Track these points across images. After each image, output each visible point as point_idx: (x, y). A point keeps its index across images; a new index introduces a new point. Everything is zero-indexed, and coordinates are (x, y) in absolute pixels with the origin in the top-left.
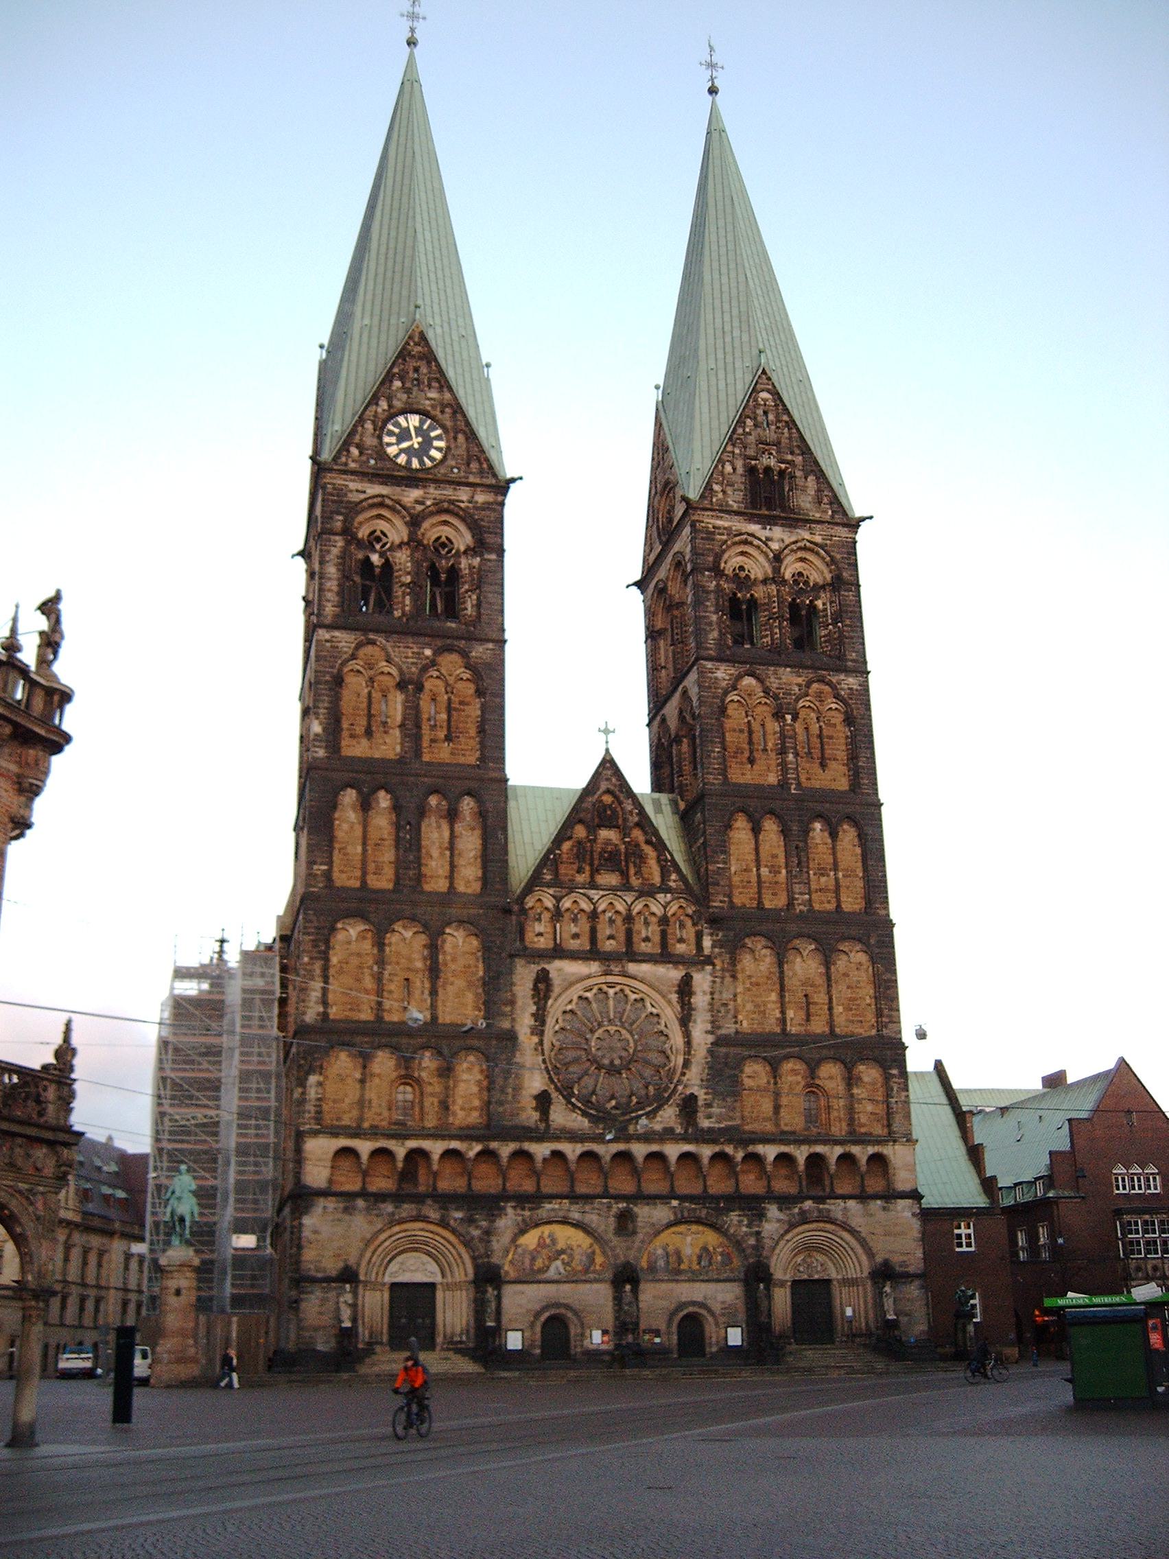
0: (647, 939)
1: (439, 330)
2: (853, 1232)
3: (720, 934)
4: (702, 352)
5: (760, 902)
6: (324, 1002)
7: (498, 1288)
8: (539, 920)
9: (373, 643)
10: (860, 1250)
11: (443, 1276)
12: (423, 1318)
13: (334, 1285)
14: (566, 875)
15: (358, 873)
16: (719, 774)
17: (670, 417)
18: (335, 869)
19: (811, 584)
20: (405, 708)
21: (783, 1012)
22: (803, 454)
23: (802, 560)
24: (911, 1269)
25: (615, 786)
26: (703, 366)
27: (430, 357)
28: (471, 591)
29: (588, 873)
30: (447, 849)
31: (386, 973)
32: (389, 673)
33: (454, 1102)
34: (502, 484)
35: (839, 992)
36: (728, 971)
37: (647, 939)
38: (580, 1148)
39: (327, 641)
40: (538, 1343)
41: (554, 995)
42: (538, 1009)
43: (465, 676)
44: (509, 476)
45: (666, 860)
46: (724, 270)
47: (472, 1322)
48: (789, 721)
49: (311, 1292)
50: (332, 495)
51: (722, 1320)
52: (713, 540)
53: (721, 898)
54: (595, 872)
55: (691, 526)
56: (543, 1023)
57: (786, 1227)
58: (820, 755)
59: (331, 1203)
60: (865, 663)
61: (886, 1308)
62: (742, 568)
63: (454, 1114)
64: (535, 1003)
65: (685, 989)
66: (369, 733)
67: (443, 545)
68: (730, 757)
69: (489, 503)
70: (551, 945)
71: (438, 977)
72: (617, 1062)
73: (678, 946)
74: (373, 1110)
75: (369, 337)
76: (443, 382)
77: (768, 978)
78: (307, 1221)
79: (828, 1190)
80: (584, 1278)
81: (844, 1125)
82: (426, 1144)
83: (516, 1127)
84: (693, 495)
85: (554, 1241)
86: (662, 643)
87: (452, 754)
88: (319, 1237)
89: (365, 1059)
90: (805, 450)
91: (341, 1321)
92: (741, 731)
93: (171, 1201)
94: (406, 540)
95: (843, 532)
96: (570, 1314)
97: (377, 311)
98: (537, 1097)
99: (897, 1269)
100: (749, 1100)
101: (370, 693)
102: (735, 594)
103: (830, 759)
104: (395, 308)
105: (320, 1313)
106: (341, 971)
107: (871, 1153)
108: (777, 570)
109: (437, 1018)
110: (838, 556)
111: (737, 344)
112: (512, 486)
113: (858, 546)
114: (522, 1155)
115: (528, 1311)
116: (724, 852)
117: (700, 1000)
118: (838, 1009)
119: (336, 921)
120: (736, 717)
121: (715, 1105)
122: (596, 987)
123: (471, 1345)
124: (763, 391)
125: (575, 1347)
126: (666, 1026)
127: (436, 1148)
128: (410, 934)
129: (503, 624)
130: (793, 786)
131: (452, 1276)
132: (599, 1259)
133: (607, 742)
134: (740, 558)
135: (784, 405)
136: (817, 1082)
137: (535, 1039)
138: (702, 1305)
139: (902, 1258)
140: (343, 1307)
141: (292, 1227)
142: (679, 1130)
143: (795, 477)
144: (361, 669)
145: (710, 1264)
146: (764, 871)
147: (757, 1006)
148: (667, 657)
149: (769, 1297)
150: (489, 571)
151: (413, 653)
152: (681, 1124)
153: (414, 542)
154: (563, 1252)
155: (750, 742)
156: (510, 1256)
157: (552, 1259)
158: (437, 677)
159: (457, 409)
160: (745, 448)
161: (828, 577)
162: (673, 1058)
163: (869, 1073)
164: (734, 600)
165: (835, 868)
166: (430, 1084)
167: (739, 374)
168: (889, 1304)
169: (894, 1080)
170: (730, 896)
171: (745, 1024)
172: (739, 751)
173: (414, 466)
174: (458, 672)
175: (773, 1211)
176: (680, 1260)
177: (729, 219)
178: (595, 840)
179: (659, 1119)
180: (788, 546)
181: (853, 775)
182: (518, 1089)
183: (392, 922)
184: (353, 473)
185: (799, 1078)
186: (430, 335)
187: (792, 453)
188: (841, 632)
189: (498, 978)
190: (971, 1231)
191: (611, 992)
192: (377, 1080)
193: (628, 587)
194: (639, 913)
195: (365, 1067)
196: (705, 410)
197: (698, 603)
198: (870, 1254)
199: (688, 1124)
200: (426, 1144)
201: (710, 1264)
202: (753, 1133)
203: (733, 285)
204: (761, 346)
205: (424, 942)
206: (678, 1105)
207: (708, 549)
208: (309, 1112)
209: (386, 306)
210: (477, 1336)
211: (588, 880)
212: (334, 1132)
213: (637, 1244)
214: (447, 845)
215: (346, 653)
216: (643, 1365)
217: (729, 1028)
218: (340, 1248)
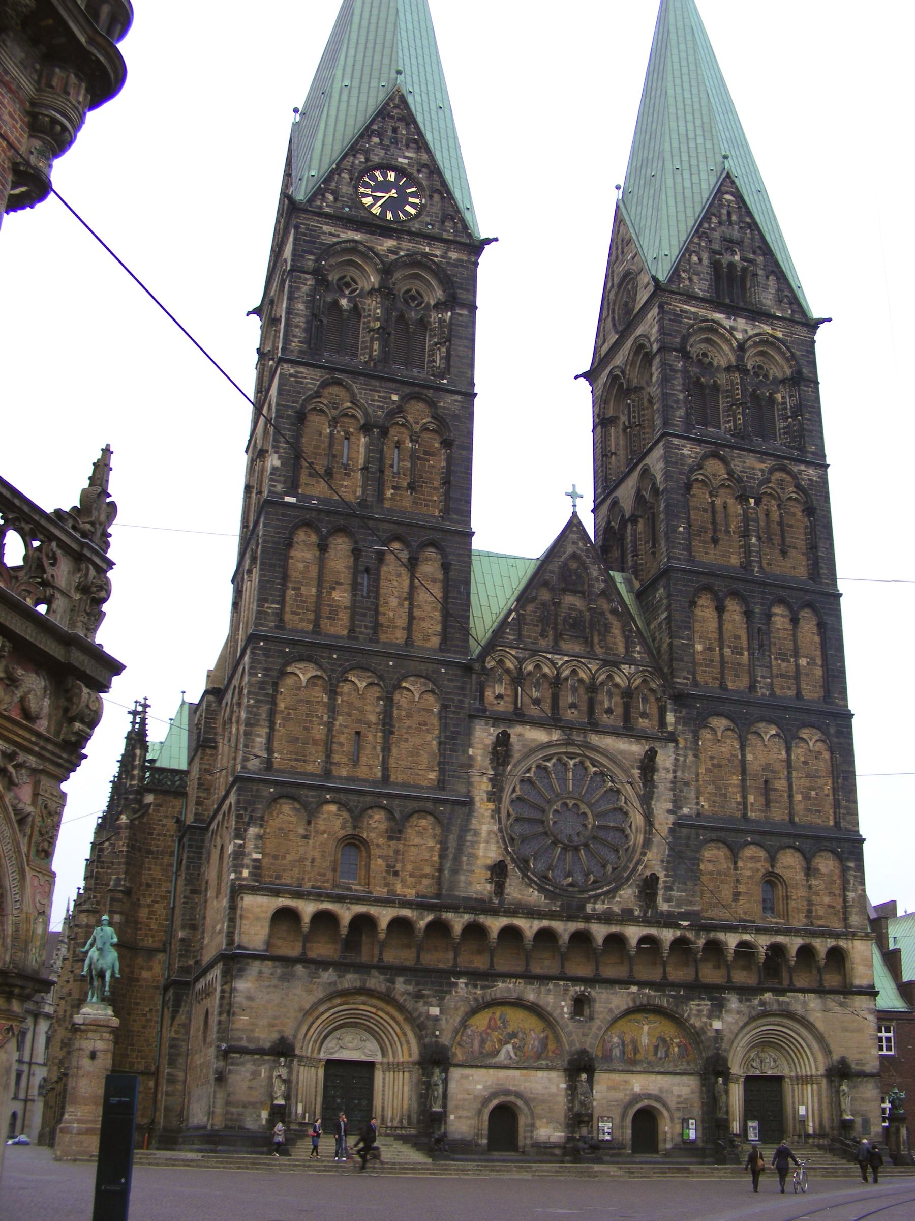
0: (609, 711)
1: (418, 98)
2: (809, 1026)
3: (684, 711)
4: (667, 156)
6: (270, 750)
7: (446, 1071)
8: (500, 681)
9: (339, 383)
10: (815, 1046)
11: (384, 1055)
12: (360, 1099)
13: (266, 1058)
14: (530, 637)
15: (311, 616)
16: (683, 550)
17: (633, 213)
18: (287, 609)
19: (771, 378)
20: (368, 451)
21: (744, 797)
22: (764, 255)
24: (868, 1069)
25: (582, 550)
26: (668, 165)
27: (409, 120)
28: (440, 343)
29: (551, 637)
30: (405, 599)
31: (337, 723)
32: (353, 416)
33: (403, 866)
34: (477, 243)
35: (800, 781)
36: (691, 749)
37: (609, 711)
38: (537, 925)
39: (291, 375)
40: (485, 1132)
41: (514, 761)
42: (496, 775)
43: (432, 427)
44: (483, 237)
45: (631, 631)
46: (686, 86)
47: (415, 1106)
49: (243, 1064)
50: (305, 235)
51: (678, 1115)
52: (681, 322)
53: (685, 674)
54: (558, 637)
55: (659, 308)
56: (501, 790)
57: (745, 1019)
58: (780, 542)
59: (267, 967)
60: (824, 456)
61: (843, 1107)
62: (705, 355)
64: (493, 768)
65: (648, 765)
66: (329, 474)
67: (413, 298)
68: (694, 535)
69: (462, 261)
70: (511, 708)
71: (392, 733)
72: (576, 839)
73: (641, 720)
75: (349, 97)
76: (421, 144)
77: (729, 760)
78: (243, 985)
79: (786, 983)
81: (802, 916)
82: (373, 910)
83: (469, 899)
84: (662, 276)
86: (612, 430)
87: (414, 503)
88: (253, 1004)
89: (310, 813)
90: (766, 250)
91: (272, 1098)
92: (705, 510)
93: (90, 954)
94: (377, 286)
95: (802, 332)
96: (520, 1103)
97: (357, 74)
99: (853, 1066)
101: (331, 432)
102: (698, 379)
103: (790, 547)
104: (375, 74)
105: (250, 1088)
106: (287, 719)
107: (829, 946)
108: (740, 358)
109: (388, 777)
110: (798, 353)
111: (701, 150)
112: (486, 247)
113: (816, 345)
114: (475, 931)
115: (476, 1097)
116: (689, 628)
117: (663, 777)
118: (798, 797)
119: (288, 664)
120: (701, 496)
121: (675, 888)
123: (413, 1131)
124: (727, 193)
125: (525, 1138)
126: (625, 803)
127: (385, 916)
128: (365, 684)
129: (472, 378)
130: (756, 569)
131: (394, 1057)
132: (552, 1046)
133: (574, 506)
134: (703, 346)
135: (747, 208)
137: (491, 806)
138: (657, 1099)
139: (857, 1056)
140: (276, 1082)
141: (223, 991)
142: (636, 913)
143: (757, 275)
144: (325, 408)
145: (667, 1055)
146: (727, 651)
147: (718, 788)
148: (617, 444)
149: (727, 1092)
150: (462, 326)
151: (379, 397)
152: (641, 906)
153: (385, 291)
154: (514, 1035)
155: (714, 522)
156: (458, 1038)
157: (503, 1043)
158: (403, 425)
159: (434, 170)
160: (710, 241)
161: (788, 372)
162: (632, 837)
163: (826, 864)
164: (698, 382)
165: (796, 655)
167: (704, 176)
168: (846, 1103)
169: (851, 872)
170: (694, 674)
171: (706, 807)
172: (703, 529)
173: (388, 218)
175: (734, 1003)
176: (636, 1050)
177: (690, 44)
178: (559, 603)
179: (617, 899)
180: (750, 338)
181: (813, 564)
183: (347, 671)
184: (327, 216)
186: (410, 100)
187: (754, 253)
188: (801, 424)
189: (454, 738)
190: (891, 1035)
191: (572, 762)
193: (576, 377)
194: (602, 684)
196: (671, 202)
197: (665, 380)
198: (827, 1051)
199: (648, 907)
200: (373, 910)
201: (667, 1055)
203: (696, 99)
204: (724, 153)
205: (378, 695)
206: (638, 887)
207: (677, 331)
208: (247, 868)
209: (367, 71)
210: (419, 1121)
211: (551, 644)
212: (276, 893)
213: (594, 1029)
214: (405, 595)
215: (310, 389)
216: (600, 1161)
218: (275, 1018)
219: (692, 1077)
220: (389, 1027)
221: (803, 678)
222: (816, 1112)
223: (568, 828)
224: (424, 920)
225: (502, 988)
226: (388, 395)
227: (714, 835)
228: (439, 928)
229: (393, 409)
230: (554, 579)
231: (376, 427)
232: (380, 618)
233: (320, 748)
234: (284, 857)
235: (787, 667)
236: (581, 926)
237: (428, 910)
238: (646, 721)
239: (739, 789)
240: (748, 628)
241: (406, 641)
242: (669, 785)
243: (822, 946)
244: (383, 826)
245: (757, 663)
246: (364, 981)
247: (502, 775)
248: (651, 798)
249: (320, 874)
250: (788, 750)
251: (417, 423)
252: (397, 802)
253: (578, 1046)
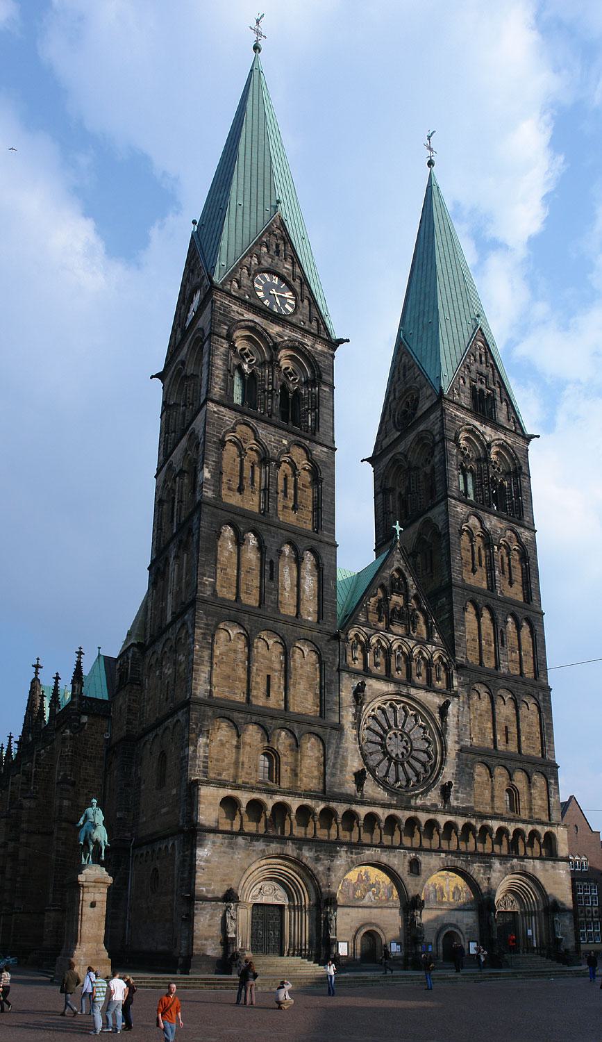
7: (335, 910)
21: (495, 736)
31: (254, 668)
33: (301, 770)
35: (523, 726)
43: (307, 467)
51: (466, 936)
54: (390, 622)
63: (301, 780)
65: (443, 710)
71: (291, 678)
74: (245, 770)
79: (522, 853)
80: (386, 905)
81: (527, 812)
82: (288, 800)
83: (342, 794)
85: (368, 877)
98: (355, 774)
100: (478, 791)
114: (350, 816)
117: (451, 721)
118: (523, 738)
121: (460, 791)
122: (389, 702)
127: (294, 803)
129: (333, 438)
136: (514, 783)
137: (355, 732)
138: (455, 926)
146: (483, 642)
152: (442, 802)
154: (373, 886)
166: (285, 756)
169: (553, 786)
175: (497, 864)
176: (443, 896)
178: (390, 600)
182: (344, 766)
185: (504, 779)
191: (398, 706)
192: (248, 748)
195: (239, 736)
200: (288, 800)
201: (460, 898)
202: (480, 812)
213: (421, 882)
217: (467, 742)
219: (473, 912)
220: (297, 882)
221: (524, 664)
222: (538, 930)
223: (395, 748)
224: (320, 807)
225: (369, 853)
227: (480, 759)
228: (328, 814)
230: (387, 583)
231: (274, 461)
232: (279, 597)
233: (245, 685)
234: (223, 761)
236: (412, 814)
237: (322, 800)
238: (440, 682)
239: (492, 731)
240: (494, 629)
241: (297, 614)
242: (455, 726)
243: (543, 830)
244: (288, 741)
246: (283, 849)
247: (360, 712)
248: (446, 733)
249: (247, 773)
250: (517, 708)
252: (296, 725)
253: (411, 893)
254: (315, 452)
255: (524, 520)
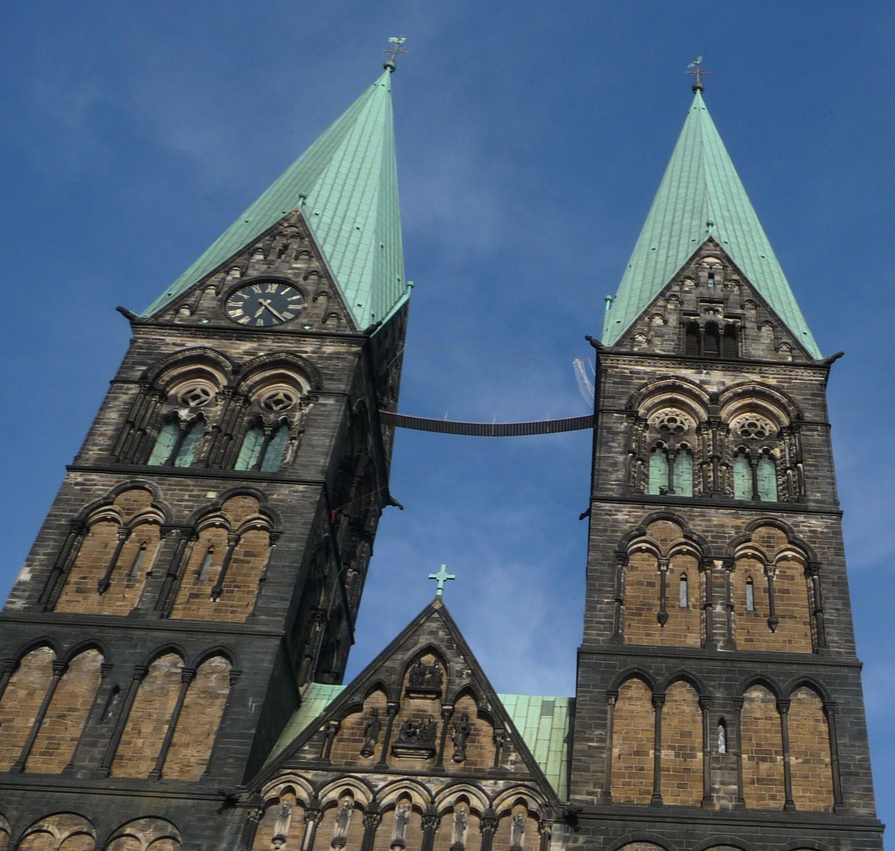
3: (581, 839)
5: (657, 795)
16: (605, 629)
19: (767, 434)
23: (752, 408)
43: (259, 523)
48: (720, 567)
68: (630, 614)
92: (651, 584)
116: (604, 726)
151: (190, 496)
174: (249, 517)
194: (449, 810)
226: (203, 494)
229: (207, 507)
235: (770, 769)
245: (715, 765)
251: (238, 521)
254: (275, 496)
255: (809, 500)
